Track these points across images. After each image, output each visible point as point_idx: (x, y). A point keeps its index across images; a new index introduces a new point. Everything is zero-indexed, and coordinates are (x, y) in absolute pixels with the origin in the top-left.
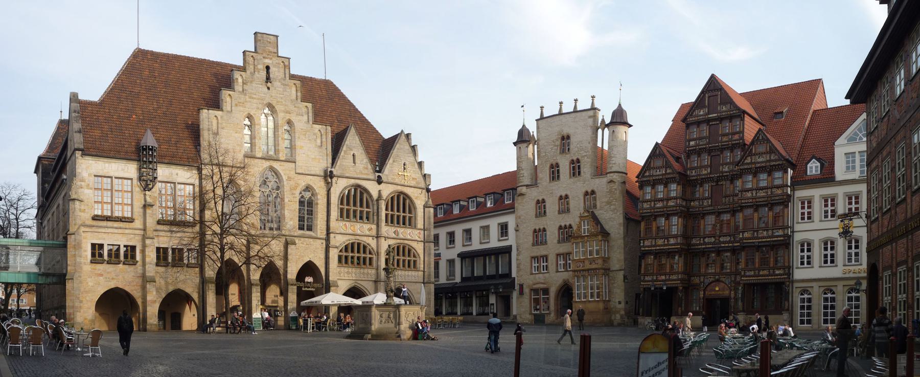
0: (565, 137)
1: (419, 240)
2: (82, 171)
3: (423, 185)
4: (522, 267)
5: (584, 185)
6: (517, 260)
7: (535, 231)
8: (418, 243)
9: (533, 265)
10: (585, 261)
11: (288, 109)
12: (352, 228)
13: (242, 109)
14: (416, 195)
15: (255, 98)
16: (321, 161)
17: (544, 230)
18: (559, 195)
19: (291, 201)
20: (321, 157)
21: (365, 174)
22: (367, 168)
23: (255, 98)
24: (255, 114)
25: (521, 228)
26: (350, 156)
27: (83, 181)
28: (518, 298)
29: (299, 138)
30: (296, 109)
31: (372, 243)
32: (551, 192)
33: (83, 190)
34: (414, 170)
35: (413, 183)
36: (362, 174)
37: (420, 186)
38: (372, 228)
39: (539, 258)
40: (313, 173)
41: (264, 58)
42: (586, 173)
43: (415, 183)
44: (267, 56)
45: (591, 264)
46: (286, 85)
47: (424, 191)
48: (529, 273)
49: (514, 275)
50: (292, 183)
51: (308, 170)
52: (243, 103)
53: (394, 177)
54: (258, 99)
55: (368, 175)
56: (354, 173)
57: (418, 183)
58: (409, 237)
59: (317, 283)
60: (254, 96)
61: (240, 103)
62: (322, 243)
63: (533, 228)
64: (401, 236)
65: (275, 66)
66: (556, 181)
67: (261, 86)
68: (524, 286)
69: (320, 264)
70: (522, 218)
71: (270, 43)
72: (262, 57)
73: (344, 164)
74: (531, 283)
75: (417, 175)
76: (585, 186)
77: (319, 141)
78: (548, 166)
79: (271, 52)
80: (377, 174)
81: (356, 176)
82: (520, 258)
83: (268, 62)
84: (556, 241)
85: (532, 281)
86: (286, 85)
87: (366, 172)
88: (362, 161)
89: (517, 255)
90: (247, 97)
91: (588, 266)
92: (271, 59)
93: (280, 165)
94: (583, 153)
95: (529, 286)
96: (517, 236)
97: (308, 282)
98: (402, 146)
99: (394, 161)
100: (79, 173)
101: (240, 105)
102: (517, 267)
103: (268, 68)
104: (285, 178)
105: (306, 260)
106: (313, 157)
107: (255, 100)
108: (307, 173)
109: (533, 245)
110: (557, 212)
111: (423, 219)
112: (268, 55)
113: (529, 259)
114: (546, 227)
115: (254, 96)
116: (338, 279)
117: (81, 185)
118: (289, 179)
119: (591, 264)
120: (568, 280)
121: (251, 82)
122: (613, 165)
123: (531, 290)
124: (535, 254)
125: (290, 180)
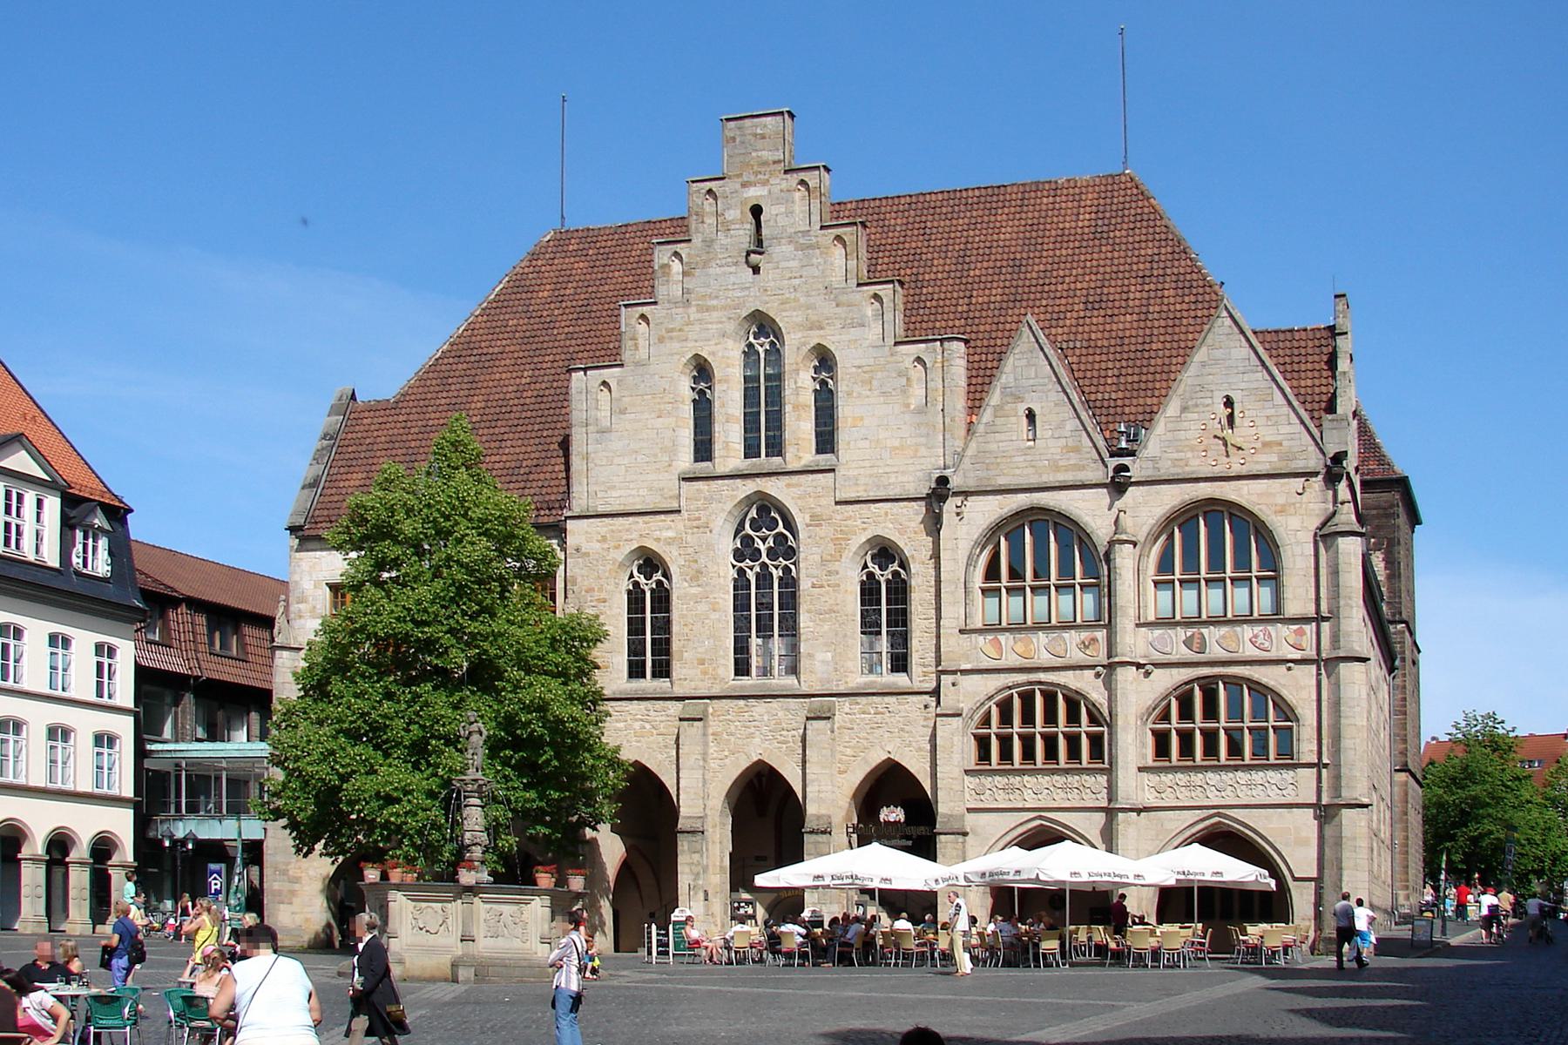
1: (1297, 655)
2: (301, 579)
3: (1314, 461)
8: (1289, 669)
11: (815, 318)
12: (1020, 648)
13: (675, 345)
14: (1281, 500)
15: (715, 308)
16: (923, 451)
19: (821, 586)
20: (923, 440)
21: (1067, 469)
22: (1077, 450)
23: (715, 308)
24: (713, 354)
26: (1013, 419)
27: (301, 600)
29: (849, 394)
30: (839, 310)
31: (1090, 686)
33: (302, 621)
34: (1272, 412)
35: (1265, 462)
36: (1057, 469)
37: (1299, 465)
38: (1094, 640)
40: (892, 494)
41: (744, 185)
43: (1274, 458)
44: (752, 178)
46: (811, 247)
47: (1317, 483)
50: (824, 531)
51: (878, 487)
52: (680, 330)
53: (1181, 455)
54: (724, 308)
55: (1083, 468)
56: (1031, 470)
57: (1288, 457)
58: (1251, 652)
59: (918, 824)
60: (715, 302)
61: (672, 330)
62: (926, 707)
64: (1215, 652)
65: (777, 202)
67: (733, 269)
69: (917, 766)
71: (763, 137)
72: (738, 186)
73: (993, 447)
75: (1285, 429)
77: (918, 392)
79: (765, 163)
80: (1113, 462)
81: (1034, 480)
83: (755, 194)
86: (811, 247)
87: (1074, 459)
88: (1060, 426)
90: (693, 309)
92: (765, 183)
93: (788, 486)
97: (887, 823)
98: (1218, 353)
99: (1184, 409)
100: (296, 582)
101: (671, 338)
103: (757, 211)
104: (800, 520)
105: (877, 757)
106: (897, 443)
107: (715, 314)
108: (872, 495)
111: (1313, 580)
112: (757, 173)
115: (715, 302)
116: (969, 810)
117: (300, 611)
118: (816, 520)
121: (706, 264)
125: (817, 526)
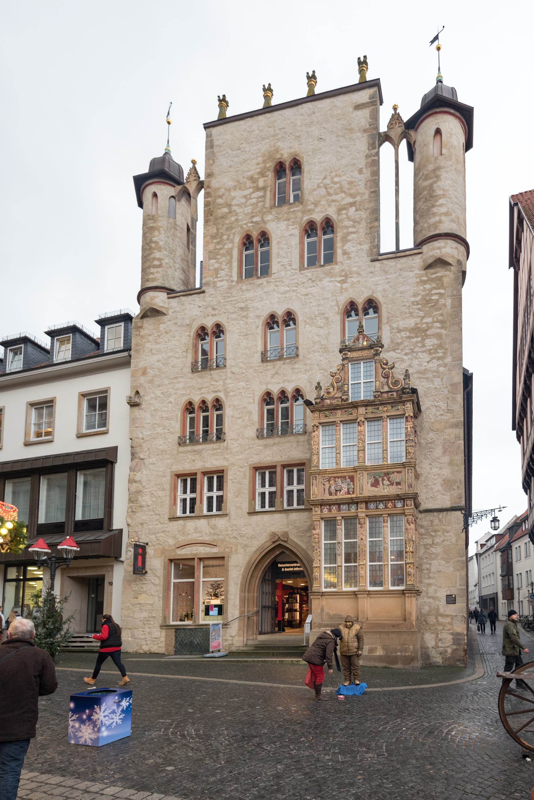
0: (287, 165)
4: (145, 499)
5: (344, 286)
6: (131, 481)
7: (189, 408)
9: (180, 495)
10: (357, 476)
17: (218, 405)
18: (265, 314)
25: (147, 399)
28: (127, 582)
32: (243, 305)
39: (199, 477)
42: (352, 255)
45: (375, 484)
48: (167, 517)
49: (117, 524)
63: (184, 401)
66: (258, 278)
68: (150, 551)
70: (151, 372)
74: (171, 542)
76: (346, 290)
78: (238, 239)
82: (138, 476)
84: (252, 432)
85: (174, 537)
89: (132, 469)
91: (368, 491)
94: (343, 199)
95: (164, 551)
96: (133, 421)
102: (130, 501)
109: (181, 442)
110: (258, 357)
113: (167, 481)
114: (221, 396)
119: (375, 484)
120: (286, 534)
122: (443, 218)
123: (171, 560)
124: (187, 467)
